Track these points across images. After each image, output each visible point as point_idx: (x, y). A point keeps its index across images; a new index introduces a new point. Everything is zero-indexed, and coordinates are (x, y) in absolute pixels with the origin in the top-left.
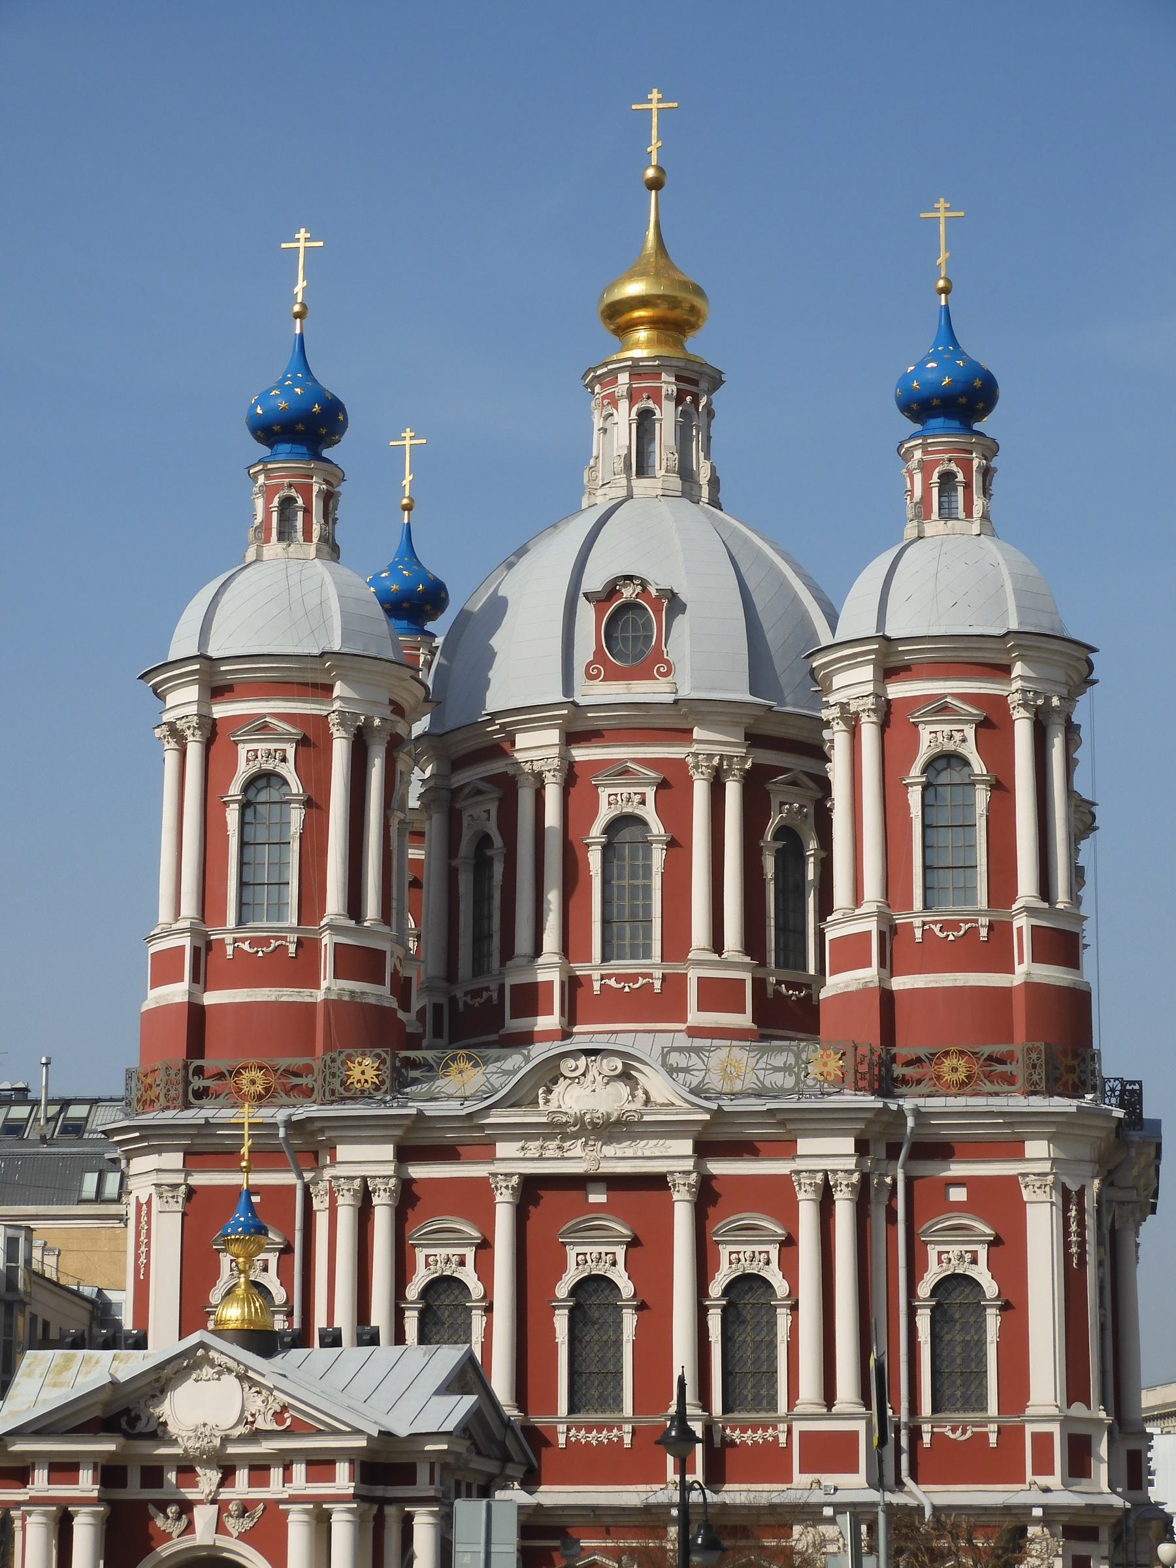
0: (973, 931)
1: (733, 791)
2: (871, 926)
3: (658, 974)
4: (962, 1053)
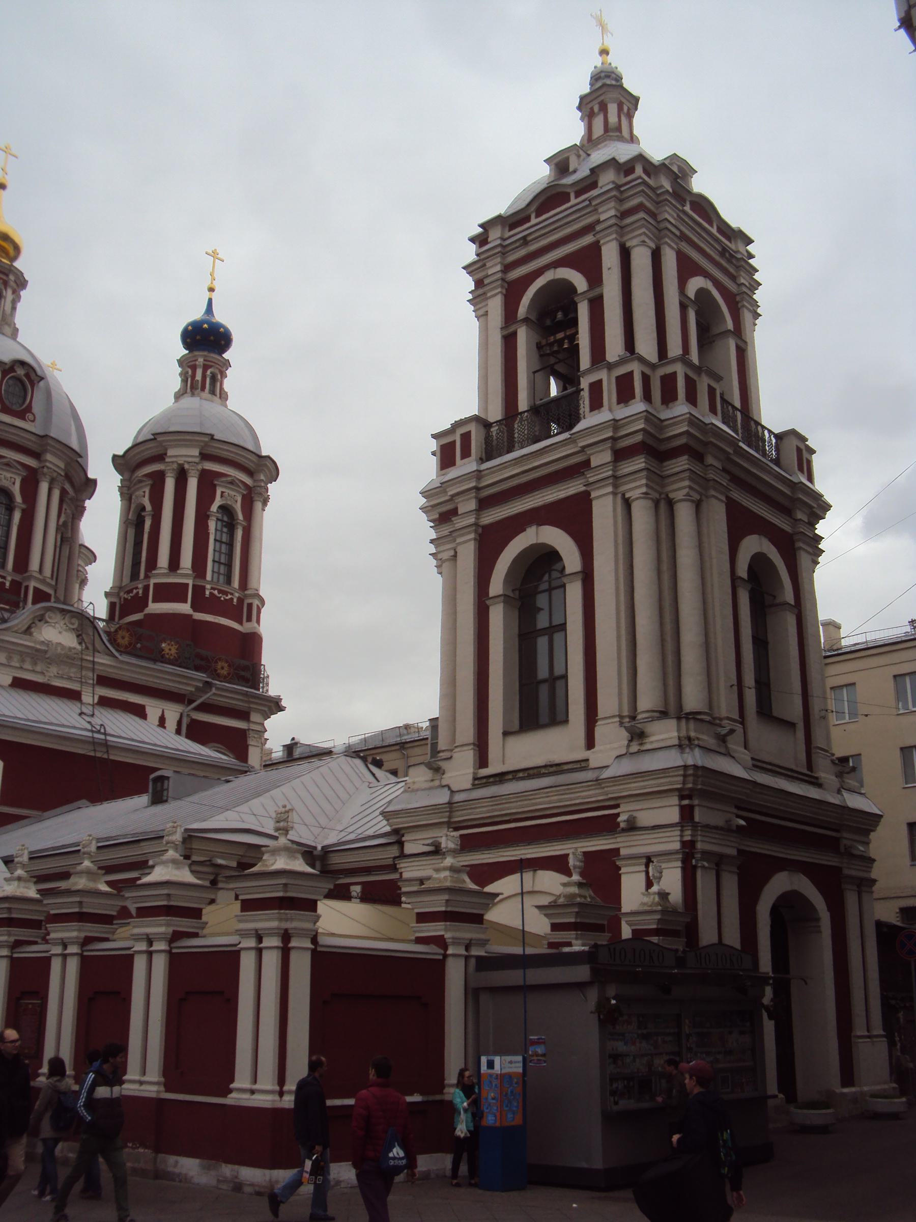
0: (232, 599)
1: (56, 494)
2: (190, 582)
3: (9, 578)
4: (227, 662)
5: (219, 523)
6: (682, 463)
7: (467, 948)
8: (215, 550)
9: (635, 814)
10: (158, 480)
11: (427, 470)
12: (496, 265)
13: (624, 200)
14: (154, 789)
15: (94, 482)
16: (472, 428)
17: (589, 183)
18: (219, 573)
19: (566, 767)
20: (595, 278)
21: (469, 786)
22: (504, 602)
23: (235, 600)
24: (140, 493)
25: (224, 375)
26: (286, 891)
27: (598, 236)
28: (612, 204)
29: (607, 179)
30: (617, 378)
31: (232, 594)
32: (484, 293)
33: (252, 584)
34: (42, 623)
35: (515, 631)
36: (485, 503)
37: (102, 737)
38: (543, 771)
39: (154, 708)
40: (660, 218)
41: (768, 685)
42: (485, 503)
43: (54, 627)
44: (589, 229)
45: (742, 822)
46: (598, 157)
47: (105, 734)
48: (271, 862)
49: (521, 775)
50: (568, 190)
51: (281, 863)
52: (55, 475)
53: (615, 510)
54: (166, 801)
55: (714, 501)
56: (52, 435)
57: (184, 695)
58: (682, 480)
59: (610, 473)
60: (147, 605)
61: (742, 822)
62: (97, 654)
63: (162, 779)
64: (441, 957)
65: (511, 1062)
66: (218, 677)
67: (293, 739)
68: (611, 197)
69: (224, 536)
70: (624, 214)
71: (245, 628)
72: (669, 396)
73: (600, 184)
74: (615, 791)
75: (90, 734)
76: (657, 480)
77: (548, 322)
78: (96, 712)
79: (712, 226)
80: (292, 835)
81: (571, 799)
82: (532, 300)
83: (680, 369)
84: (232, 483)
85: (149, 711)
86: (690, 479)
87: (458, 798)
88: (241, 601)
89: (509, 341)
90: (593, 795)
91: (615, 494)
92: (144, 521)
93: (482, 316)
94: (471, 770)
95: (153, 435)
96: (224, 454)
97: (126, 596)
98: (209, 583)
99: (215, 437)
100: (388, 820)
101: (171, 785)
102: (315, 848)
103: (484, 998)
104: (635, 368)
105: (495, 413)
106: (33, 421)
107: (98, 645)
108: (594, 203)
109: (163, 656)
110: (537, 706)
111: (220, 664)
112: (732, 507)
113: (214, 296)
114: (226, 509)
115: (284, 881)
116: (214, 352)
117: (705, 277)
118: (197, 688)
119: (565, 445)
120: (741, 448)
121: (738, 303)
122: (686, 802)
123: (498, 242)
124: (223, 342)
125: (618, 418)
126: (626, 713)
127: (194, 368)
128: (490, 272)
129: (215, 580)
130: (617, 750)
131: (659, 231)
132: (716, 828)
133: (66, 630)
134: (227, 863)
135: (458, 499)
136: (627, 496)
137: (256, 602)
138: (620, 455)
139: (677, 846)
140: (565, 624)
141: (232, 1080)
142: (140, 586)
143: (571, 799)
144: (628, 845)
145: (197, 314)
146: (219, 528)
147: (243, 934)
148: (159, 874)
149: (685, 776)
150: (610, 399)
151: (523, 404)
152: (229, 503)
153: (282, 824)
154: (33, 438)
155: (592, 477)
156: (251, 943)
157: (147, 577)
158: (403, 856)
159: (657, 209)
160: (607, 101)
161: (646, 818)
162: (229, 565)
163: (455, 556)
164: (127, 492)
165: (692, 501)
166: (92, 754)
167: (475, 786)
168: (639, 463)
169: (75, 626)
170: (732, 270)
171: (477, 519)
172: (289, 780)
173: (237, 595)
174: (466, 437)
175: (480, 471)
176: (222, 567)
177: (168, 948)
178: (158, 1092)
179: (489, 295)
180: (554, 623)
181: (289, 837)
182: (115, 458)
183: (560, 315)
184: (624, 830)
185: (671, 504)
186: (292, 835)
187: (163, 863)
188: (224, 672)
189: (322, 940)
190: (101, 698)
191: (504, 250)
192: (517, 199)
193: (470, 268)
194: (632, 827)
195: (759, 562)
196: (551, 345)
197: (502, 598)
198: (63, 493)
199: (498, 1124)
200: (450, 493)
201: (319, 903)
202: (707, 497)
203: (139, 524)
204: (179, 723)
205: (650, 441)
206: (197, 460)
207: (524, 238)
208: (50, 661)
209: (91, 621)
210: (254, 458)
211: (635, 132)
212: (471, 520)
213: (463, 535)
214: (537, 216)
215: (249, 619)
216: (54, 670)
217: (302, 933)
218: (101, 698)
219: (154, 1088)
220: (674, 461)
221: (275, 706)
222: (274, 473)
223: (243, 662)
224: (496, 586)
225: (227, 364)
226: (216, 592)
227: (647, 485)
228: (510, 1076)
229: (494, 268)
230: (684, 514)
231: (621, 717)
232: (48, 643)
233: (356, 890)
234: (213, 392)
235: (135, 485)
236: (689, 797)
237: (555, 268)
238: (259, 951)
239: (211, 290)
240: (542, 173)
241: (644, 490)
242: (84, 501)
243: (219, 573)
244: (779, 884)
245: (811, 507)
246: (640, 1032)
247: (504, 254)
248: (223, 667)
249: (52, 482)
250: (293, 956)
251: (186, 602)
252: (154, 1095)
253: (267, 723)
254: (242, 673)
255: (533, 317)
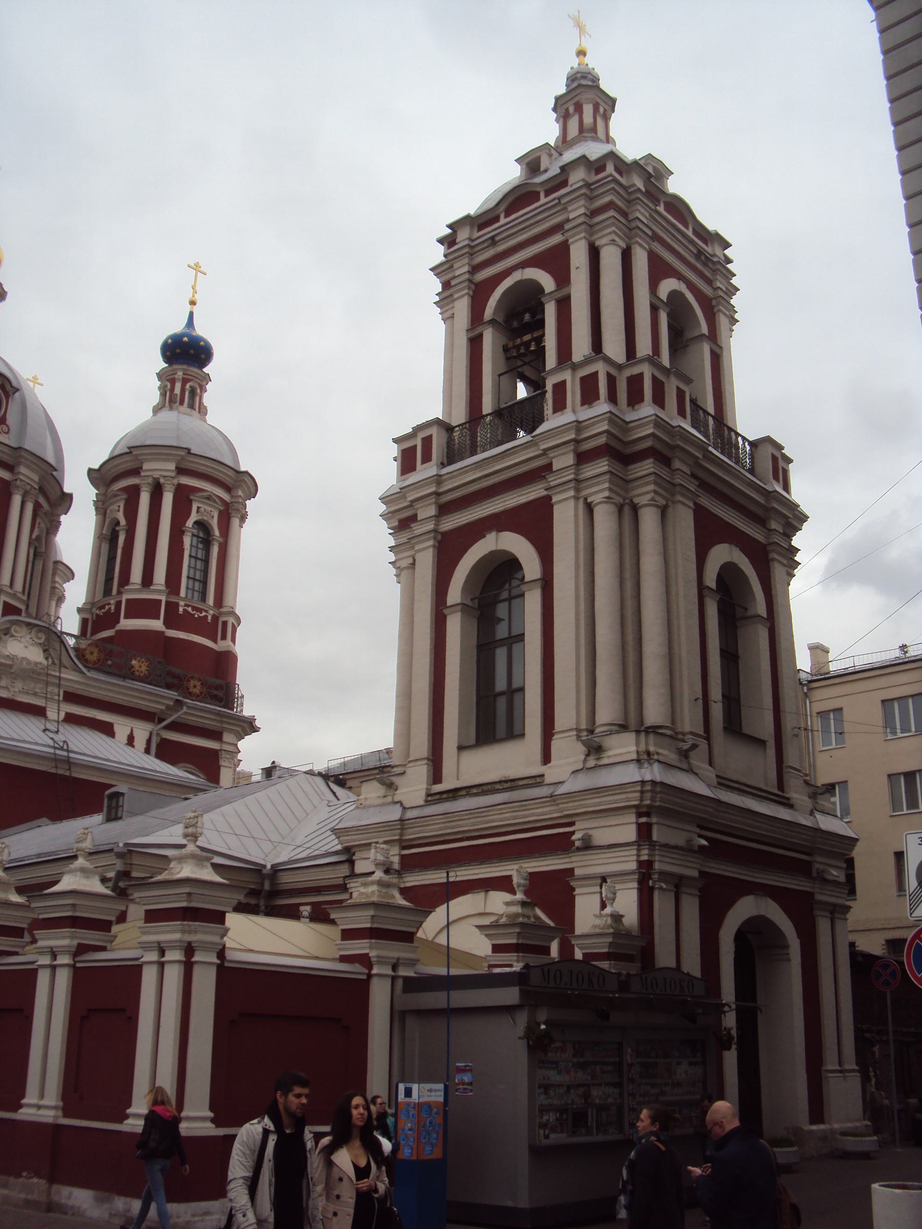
0: (206, 617)
1: (30, 507)
2: (163, 598)
4: (200, 680)
5: (195, 539)
6: (647, 466)
7: (395, 968)
8: (189, 567)
9: (590, 832)
10: (133, 494)
11: (388, 475)
12: (464, 265)
13: (596, 197)
14: (110, 808)
15: (70, 497)
16: (434, 431)
17: (559, 182)
18: (193, 590)
19: (521, 783)
20: (563, 278)
21: (422, 803)
22: (462, 611)
23: (210, 618)
24: (115, 507)
25: (203, 389)
26: (190, 901)
27: (567, 235)
28: (582, 202)
29: (577, 177)
30: (582, 379)
31: (206, 611)
32: (451, 295)
33: (228, 601)
34: (8, 636)
35: (474, 641)
36: (444, 509)
37: (65, 754)
38: (498, 786)
39: (122, 726)
40: (631, 217)
41: (738, 701)
42: (444, 509)
43: (20, 641)
44: (558, 228)
45: (704, 842)
46: (570, 156)
47: (68, 751)
48: (178, 870)
49: (475, 791)
50: (538, 189)
51: (187, 871)
52: (28, 487)
53: (576, 515)
54: (121, 818)
55: (680, 506)
56: (26, 447)
57: (153, 714)
58: (647, 484)
59: (572, 476)
60: (118, 622)
61: (704, 842)
62: (63, 670)
63: (118, 795)
64: (365, 977)
65: (430, 1090)
66: (190, 695)
67: (274, 762)
68: (582, 195)
69: (200, 551)
70: (594, 213)
71: (221, 646)
72: (635, 398)
73: (570, 182)
74: (570, 808)
75: (52, 751)
76: (621, 485)
77: (515, 324)
78: (61, 728)
79: (687, 228)
80: (201, 842)
81: (525, 816)
82: (499, 301)
83: (647, 371)
84: (208, 498)
85: (117, 729)
86: (655, 483)
87: (410, 814)
88: (215, 618)
89: (475, 343)
90: (548, 812)
91: (576, 498)
92: (117, 537)
93: (448, 318)
94: (425, 786)
95: (129, 448)
96: (201, 469)
97: (98, 612)
98: (183, 599)
99: (192, 451)
100: (338, 838)
101: (126, 803)
102: (265, 866)
103: (410, 1022)
104: (600, 368)
105: (459, 417)
106: (7, 433)
107: (65, 659)
108: (563, 202)
109: (133, 673)
110: (493, 719)
111: (192, 682)
112: (700, 514)
113: (195, 309)
114: (201, 525)
115: (187, 890)
116: (194, 366)
117: (679, 279)
118: (168, 707)
119: (526, 448)
120: (711, 453)
121: (713, 307)
122: (643, 820)
123: (466, 242)
124: (203, 356)
125: (581, 420)
126: (583, 726)
127: (173, 382)
128: (457, 273)
129: (190, 596)
130: (583, 768)
131: (630, 230)
132: (676, 847)
133: (32, 645)
134: (130, 873)
135: (417, 505)
136: (589, 500)
137: (231, 620)
138: (583, 458)
139: (633, 866)
140: (523, 634)
141: (129, 1105)
142: (112, 602)
143: (525, 816)
144: (584, 865)
145: (177, 326)
146: (194, 543)
147: (146, 947)
148: (67, 883)
149: (642, 792)
150: (573, 402)
151: (487, 406)
152: (205, 518)
153: (190, 830)
154: (6, 450)
155: (553, 480)
156: (153, 956)
157: (119, 593)
158: (353, 875)
159: (628, 208)
160: (584, 101)
161: (602, 837)
162: (204, 582)
163: (414, 564)
164: (102, 507)
165: (657, 506)
166: (53, 771)
167: (428, 803)
168: (602, 466)
169: (41, 641)
170: (707, 274)
171: (437, 525)
172: (243, 796)
173: (211, 612)
174: (427, 441)
175: (440, 476)
176: (197, 584)
177: (72, 962)
178: (56, 1117)
179: (456, 296)
180: (513, 634)
181: (198, 843)
182: (90, 471)
183: (527, 317)
184: (578, 849)
185: (635, 509)
186: (201, 842)
187: (71, 872)
188: (197, 691)
189: (230, 955)
190: (67, 714)
191: (472, 250)
192: (487, 200)
193: (437, 270)
194: (587, 846)
195: (728, 572)
196: (518, 347)
197: (459, 607)
198: (37, 507)
199: (414, 1158)
200: (409, 499)
201: (227, 914)
202: (674, 502)
203: (113, 539)
204: (149, 742)
205: (614, 444)
206: (173, 474)
207: (492, 238)
208: (15, 676)
209: (59, 637)
210: (231, 473)
211: (611, 134)
212: (430, 526)
213: (419, 542)
214: (506, 217)
215: (224, 637)
216: (19, 685)
217: (206, 947)
218: (67, 714)
219: (52, 1113)
220: (639, 464)
221: (249, 726)
222: (253, 489)
223: (218, 682)
224: (455, 594)
225: (207, 378)
226: (190, 609)
227: (610, 489)
228: (429, 1105)
229: (462, 269)
230: (649, 520)
231: (578, 730)
232: (12, 658)
233: (306, 910)
234: (191, 406)
235: (110, 498)
236: (648, 814)
237: (523, 268)
238: (162, 965)
239: (193, 303)
240: (513, 174)
241: (607, 494)
242: (59, 516)
243: (193, 590)
244: (745, 908)
245: (786, 517)
246: (575, 1060)
247: (472, 255)
248: (195, 686)
249: (25, 495)
250: (197, 971)
251: (158, 618)
252: (50, 1120)
253: (241, 744)
254: (215, 692)
255: (500, 320)
